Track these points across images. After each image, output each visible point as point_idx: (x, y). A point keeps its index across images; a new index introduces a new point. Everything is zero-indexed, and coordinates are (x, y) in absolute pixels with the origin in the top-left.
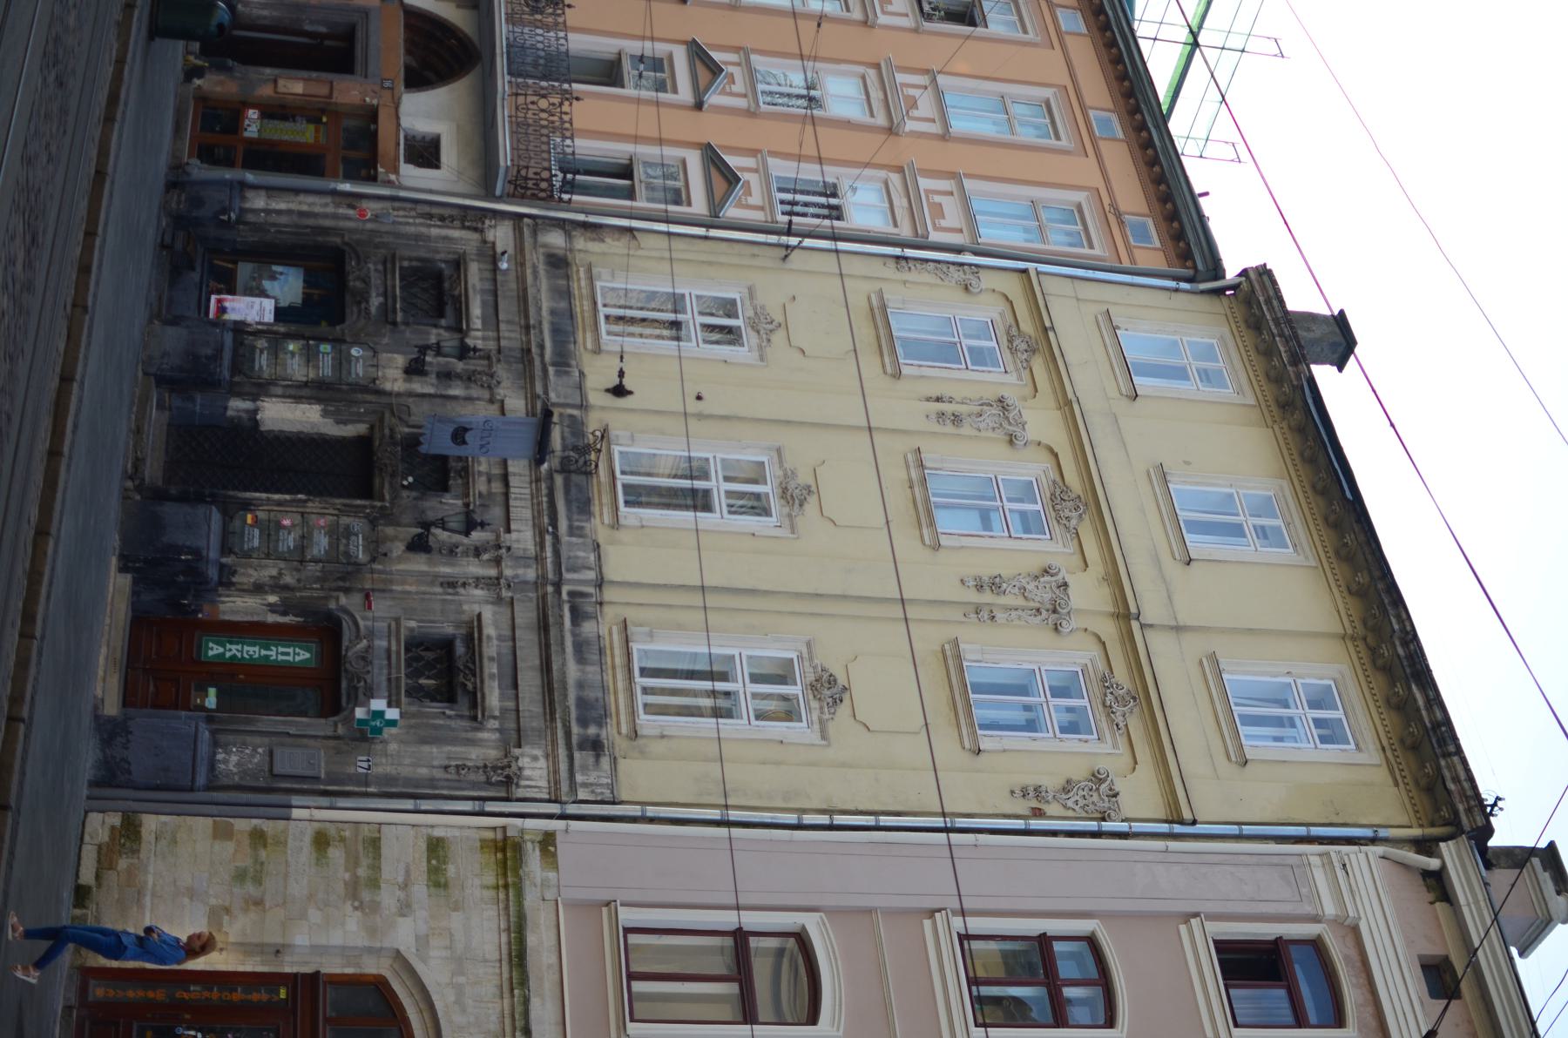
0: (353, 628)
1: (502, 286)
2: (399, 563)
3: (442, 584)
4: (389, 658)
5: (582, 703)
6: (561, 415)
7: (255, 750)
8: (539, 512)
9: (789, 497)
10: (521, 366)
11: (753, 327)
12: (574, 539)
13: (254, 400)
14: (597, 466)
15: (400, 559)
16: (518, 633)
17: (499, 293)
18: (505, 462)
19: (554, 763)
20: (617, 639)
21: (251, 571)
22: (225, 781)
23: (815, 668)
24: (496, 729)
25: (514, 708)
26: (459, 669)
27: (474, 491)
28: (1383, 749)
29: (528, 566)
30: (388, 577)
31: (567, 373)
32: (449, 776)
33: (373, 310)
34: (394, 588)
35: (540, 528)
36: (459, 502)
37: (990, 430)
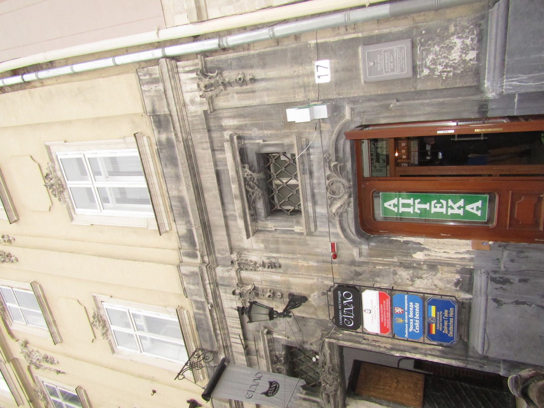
0: (345, 225)
2: (311, 285)
3: (280, 267)
4: (313, 195)
5: (173, 161)
7: (432, 71)
8: (222, 322)
9: (101, 321)
12: (198, 299)
15: (312, 288)
21: (440, 284)
24: (225, 130)
25: (216, 153)
26: (258, 186)
29: (222, 278)
30: (320, 275)
34: (315, 264)
36: (275, 336)
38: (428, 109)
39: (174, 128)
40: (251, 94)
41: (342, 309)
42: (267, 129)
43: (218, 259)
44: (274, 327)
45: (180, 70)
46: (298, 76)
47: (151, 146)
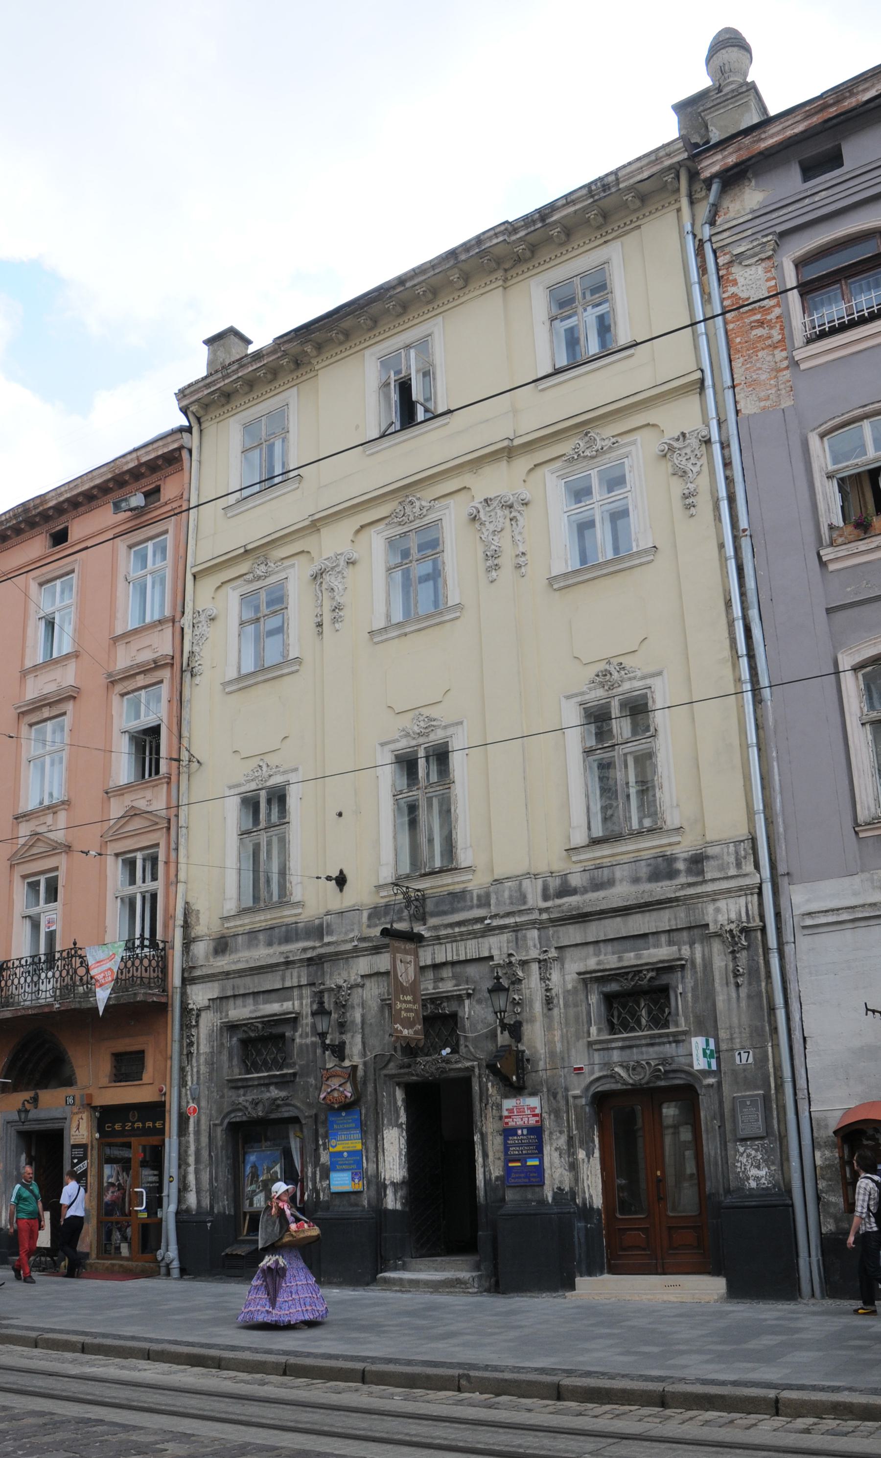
3: (550, 1009)
5: (655, 876)
6: (369, 926)
7: (742, 1155)
8: (470, 934)
10: (325, 965)
12: (493, 901)
13: (385, 1187)
14: (418, 890)
16: (591, 939)
17: (256, 990)
18: (423, 969)
19: (720, 894)
22: (778, 1177)
24: (691, 947)
26: (634, 986)
27: (456, 991)
29: (525, 938)
31: (328, 925)
32: (746, 982)
33: (283, 1094)
34: (558, 1050)
35: (485, 932)
36: (467, 1002)
37: (345, 580)
38: (712, 1153)
39: (690, 885)
40: (725, 982)
42: (692, 996)
43: (546, 930)
45: (749, 897)
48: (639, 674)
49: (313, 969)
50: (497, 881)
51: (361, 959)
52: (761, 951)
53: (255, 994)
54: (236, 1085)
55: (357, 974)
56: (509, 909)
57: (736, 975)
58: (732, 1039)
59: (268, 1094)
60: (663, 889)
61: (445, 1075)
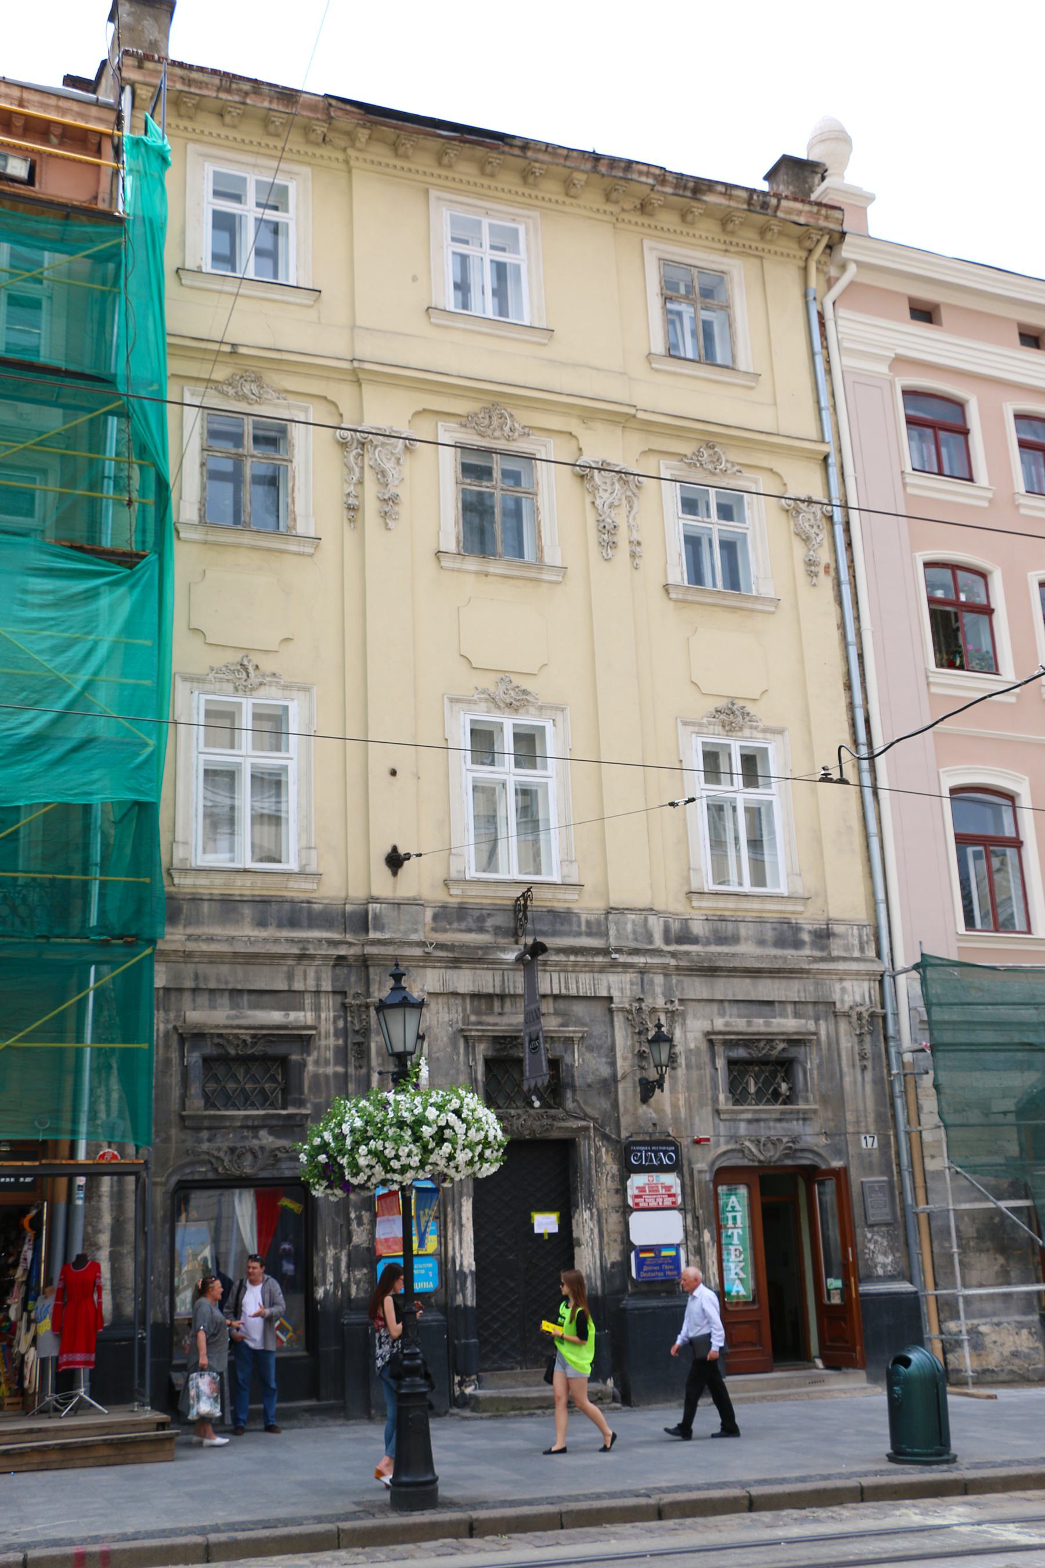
0: (729, 1155)
1: (227, 983)
2: (663, 1111)
4: (758, 1120)
5: (780, 942)
6: (434, 930)
7: (870, 1241)
8: (585, 966)
9: (518, 704)
10: (371, 970)
11: (252, 690)
12: (612, 932)
15: (659, 1111)
17: (239, 987)
19: (848, 974)
20: (707, 903)
23: (709, 723)
24: (816, 1023)
26: (765, 1055)
28: (726, 251)
31: (376, 917)
35: (604, 967)
41: (652, 1151)
44: (587, 1048)
45: (872, 983)
46: (866, 1117)
47: (793, 913)
48: (761, 725)
49: (342, 972)
50: (609, 911)
51: (429, 971)
52: (882, 1037)
53: (235, 993)
54: (188, 1124)
55: (422, 990)
56: (633, 945)
57: (863, 1057)
58: (858, 1122)
59: (255, 1142)
60: (790, 956)
61: (546, 1135)
